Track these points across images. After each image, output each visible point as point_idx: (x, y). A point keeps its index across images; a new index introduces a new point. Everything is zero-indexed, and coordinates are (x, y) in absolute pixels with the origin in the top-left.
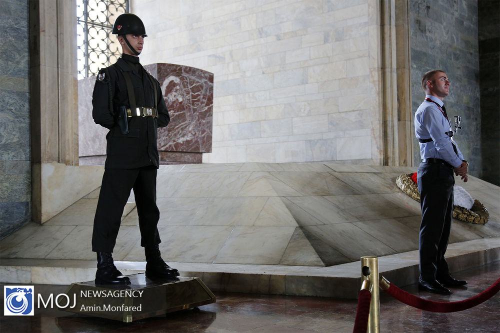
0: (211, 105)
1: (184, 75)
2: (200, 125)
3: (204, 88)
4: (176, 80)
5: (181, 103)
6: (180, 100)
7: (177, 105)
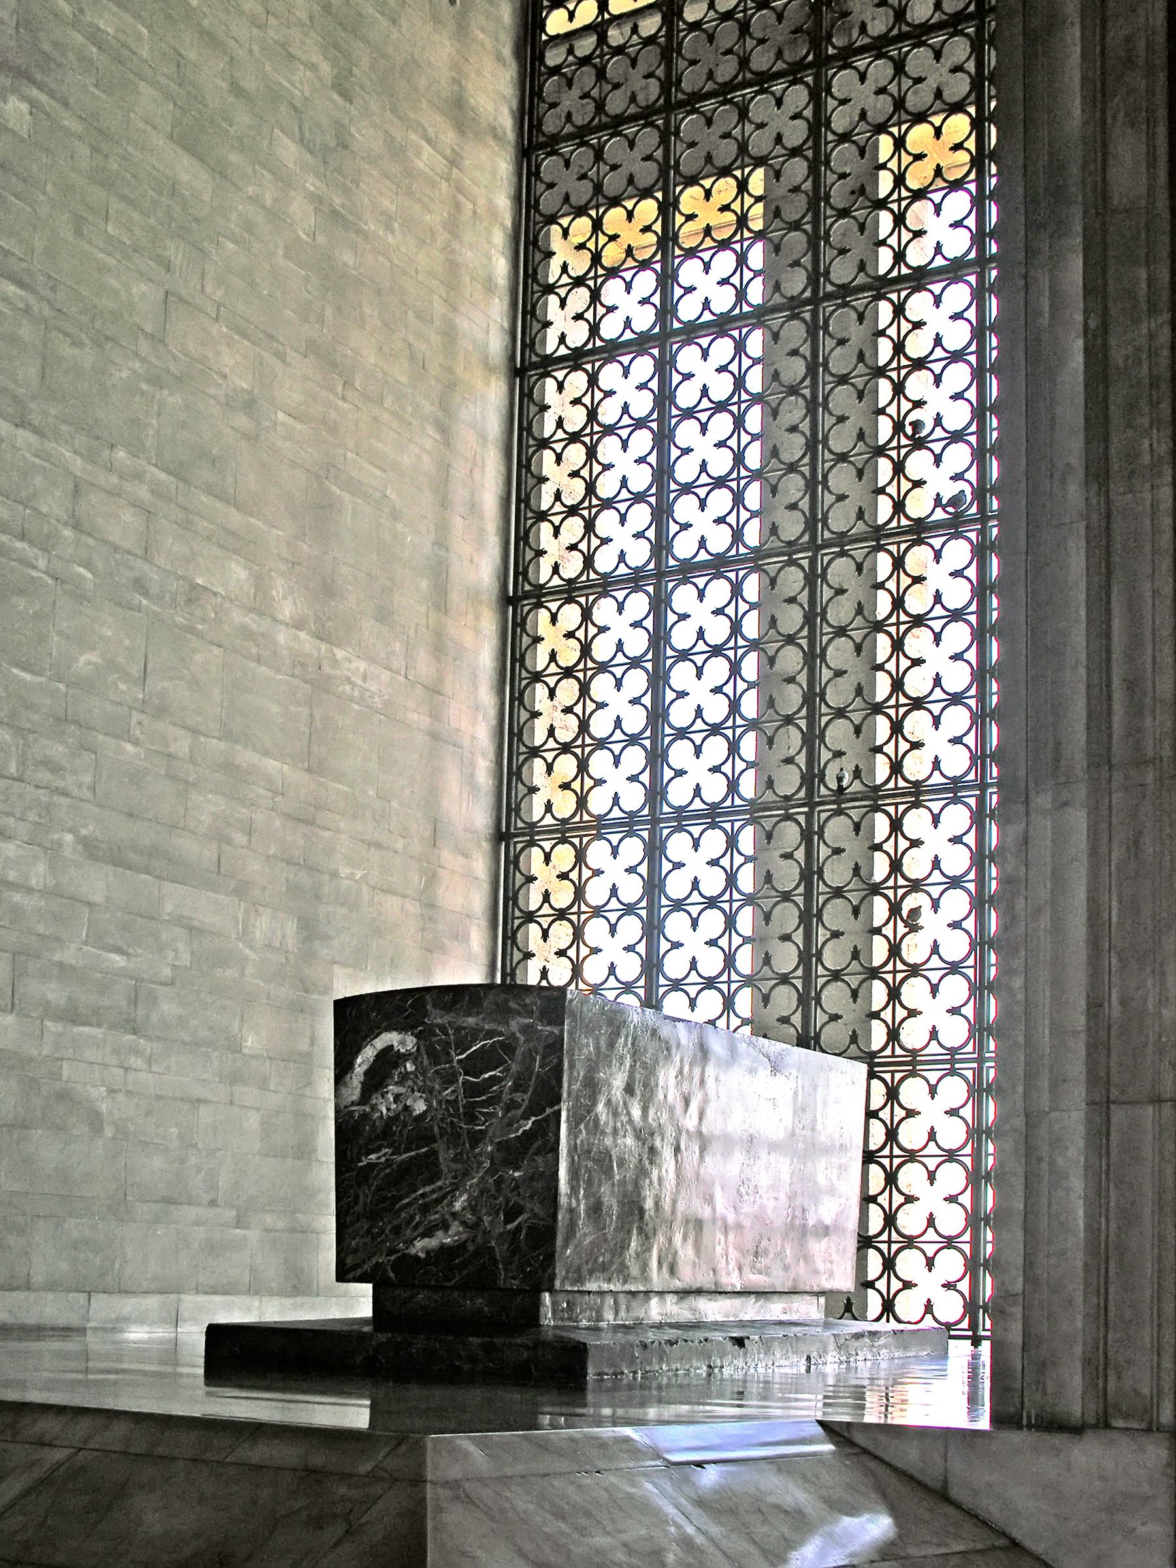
0: (548, 1111)
1: (438, 1018)
2: (499, 1190)
3: (519, 1052)
4: (403, 1043)
5: (423, 1115)
6: (420, 1107)
7: (405, 1126)
